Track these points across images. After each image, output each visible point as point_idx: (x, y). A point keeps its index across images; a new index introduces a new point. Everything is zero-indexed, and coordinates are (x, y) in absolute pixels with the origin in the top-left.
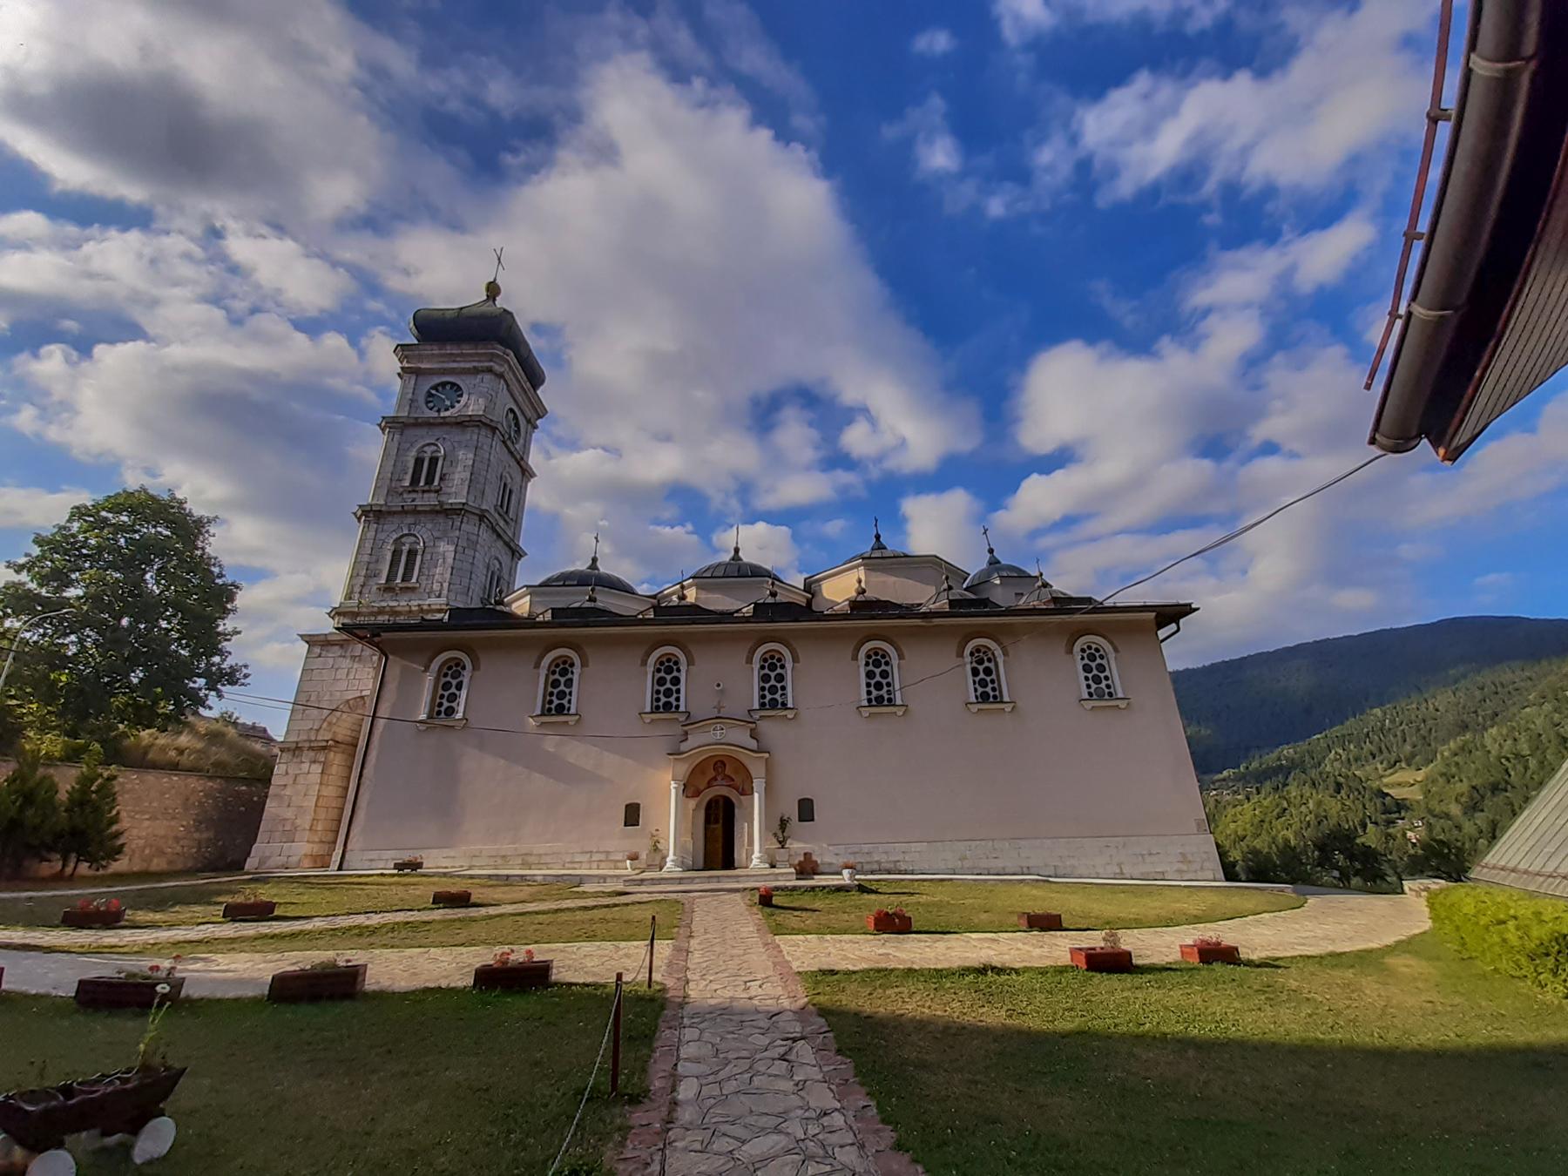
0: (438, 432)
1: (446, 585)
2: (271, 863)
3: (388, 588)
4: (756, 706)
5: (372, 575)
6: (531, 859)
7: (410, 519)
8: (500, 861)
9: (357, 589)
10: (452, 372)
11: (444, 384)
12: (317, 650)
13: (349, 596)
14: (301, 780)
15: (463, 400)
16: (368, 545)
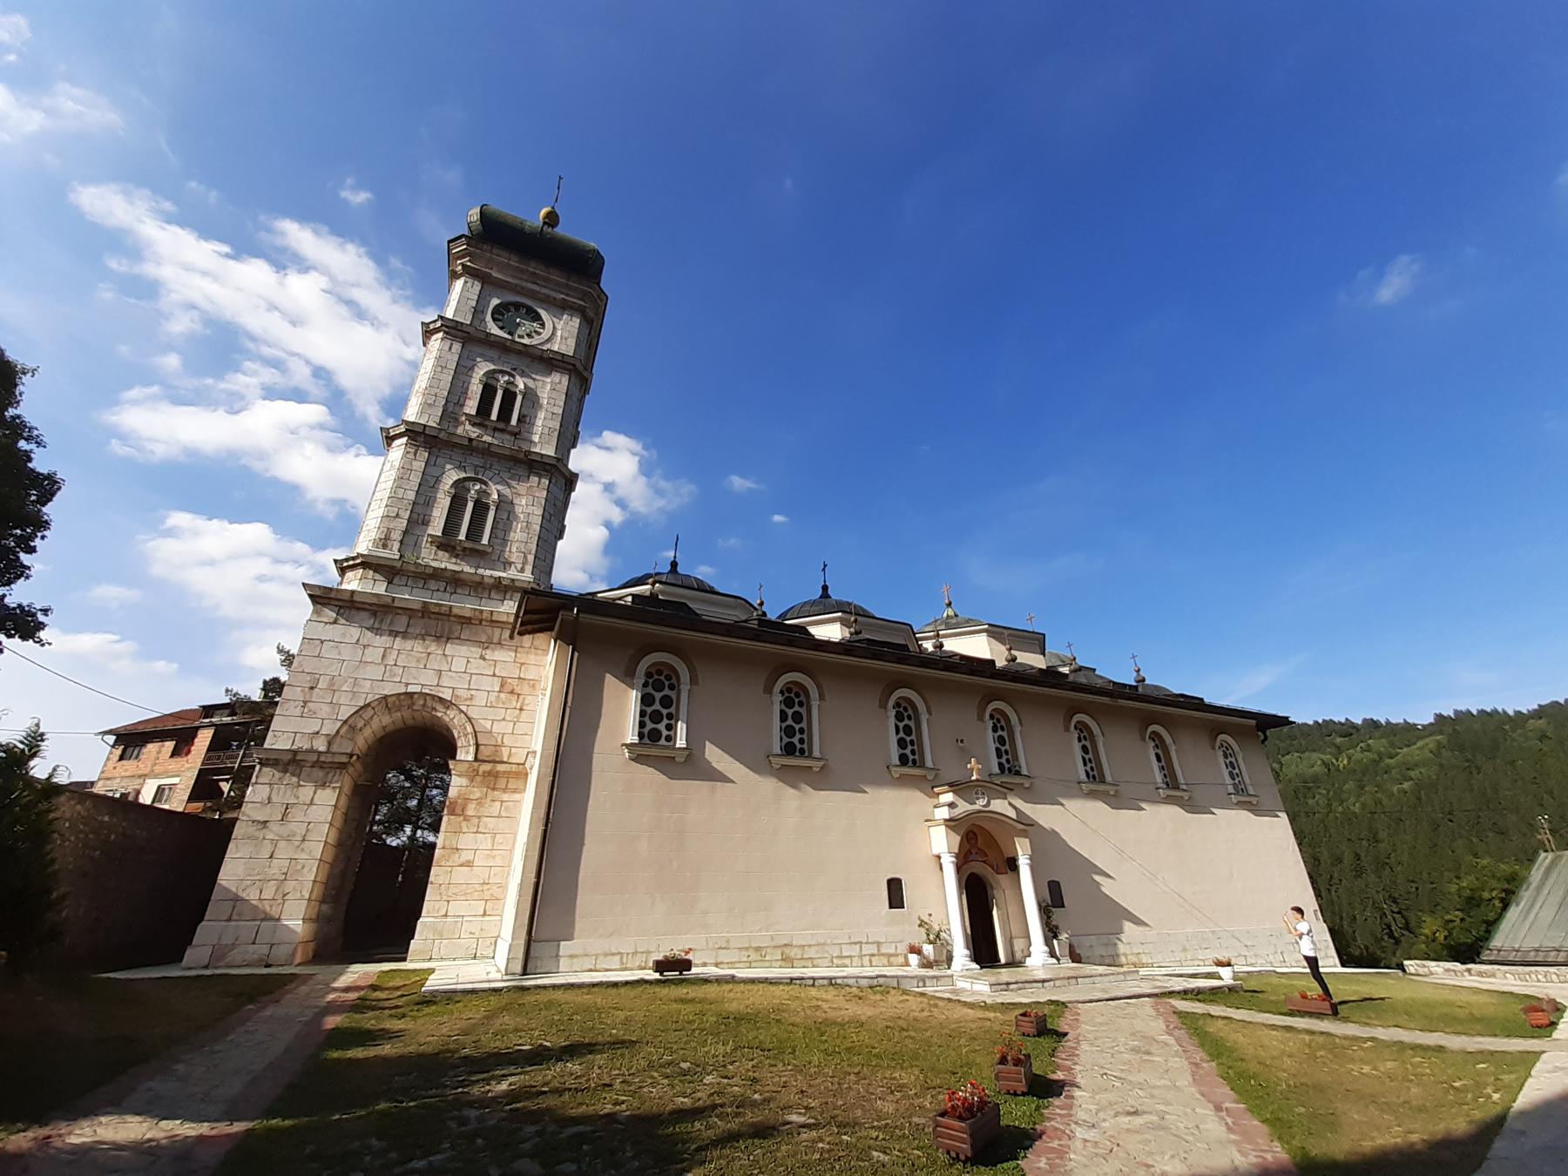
0: (515, 361)
1: (531, 558)
2: (236, 955)
3: (446, 543)
4: (996, 770)
5: (418, 519)
6: (793, 953)
7: (477, 461)
8: (754, 956)
9: (396, 536)
10: (533, 295)
11: (518, 306)
12: (330, 614)
13: (385, 542)
14: (296, 814)
15: (546, 334)
16: (415, 479)
